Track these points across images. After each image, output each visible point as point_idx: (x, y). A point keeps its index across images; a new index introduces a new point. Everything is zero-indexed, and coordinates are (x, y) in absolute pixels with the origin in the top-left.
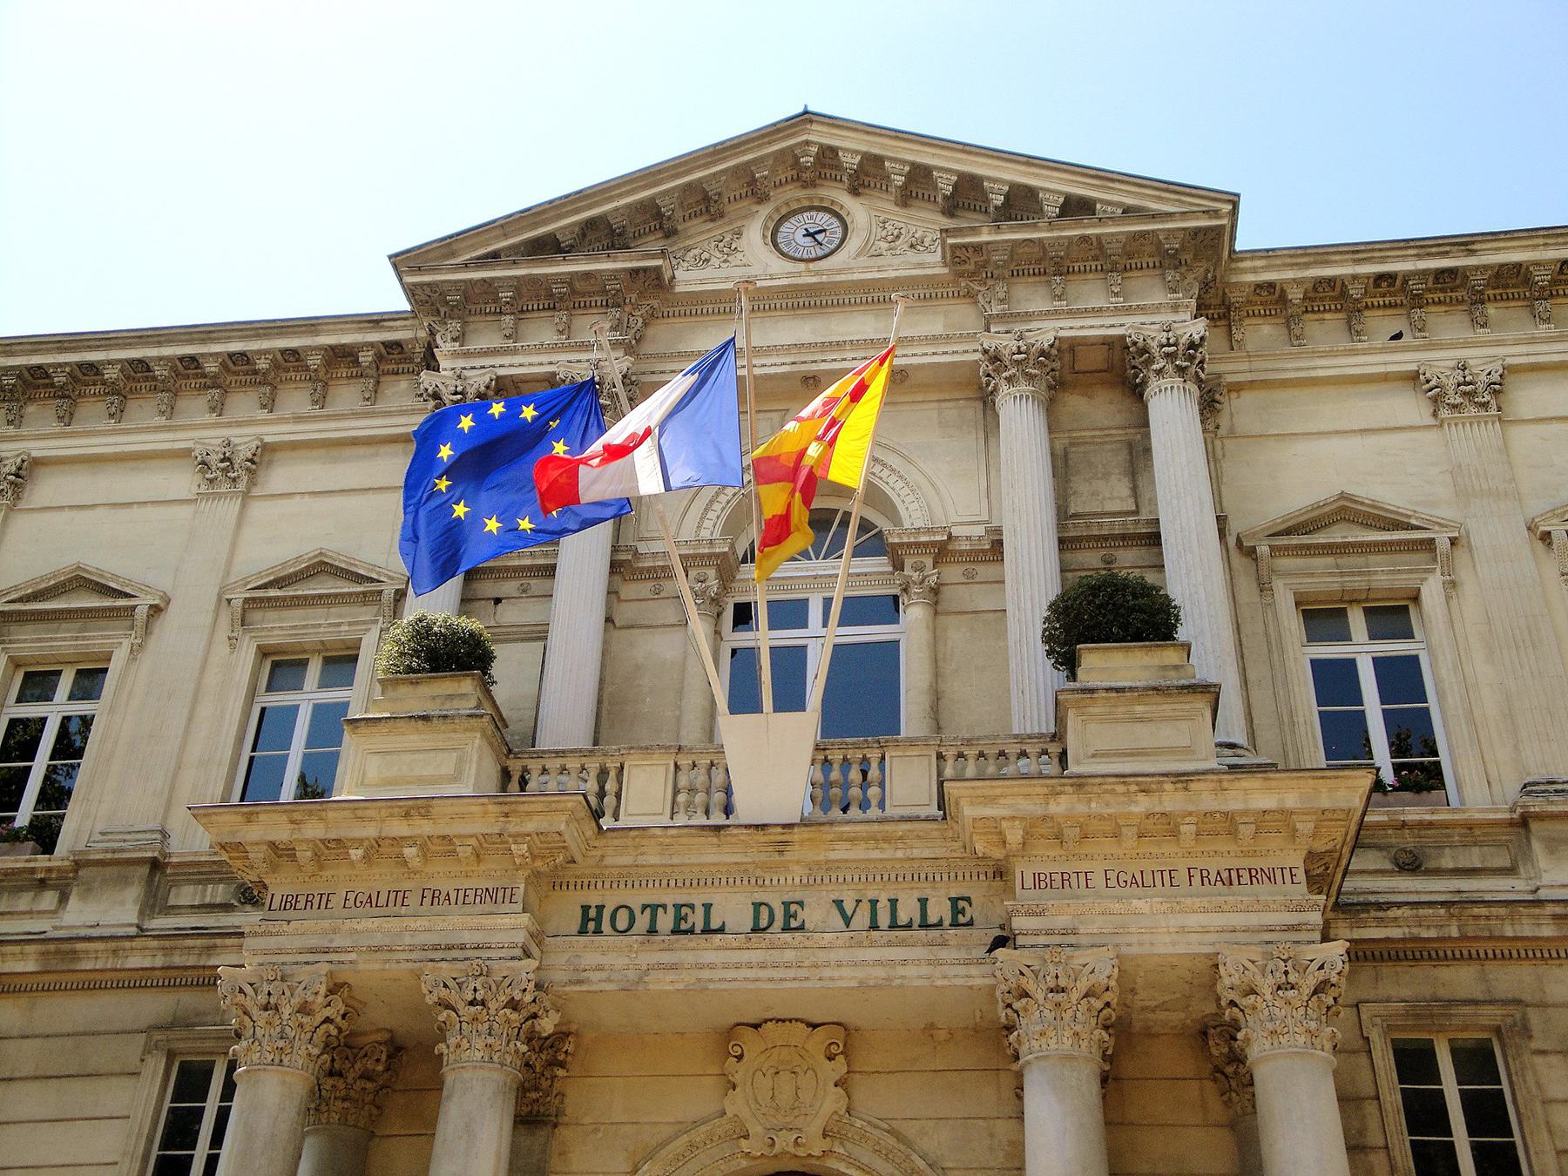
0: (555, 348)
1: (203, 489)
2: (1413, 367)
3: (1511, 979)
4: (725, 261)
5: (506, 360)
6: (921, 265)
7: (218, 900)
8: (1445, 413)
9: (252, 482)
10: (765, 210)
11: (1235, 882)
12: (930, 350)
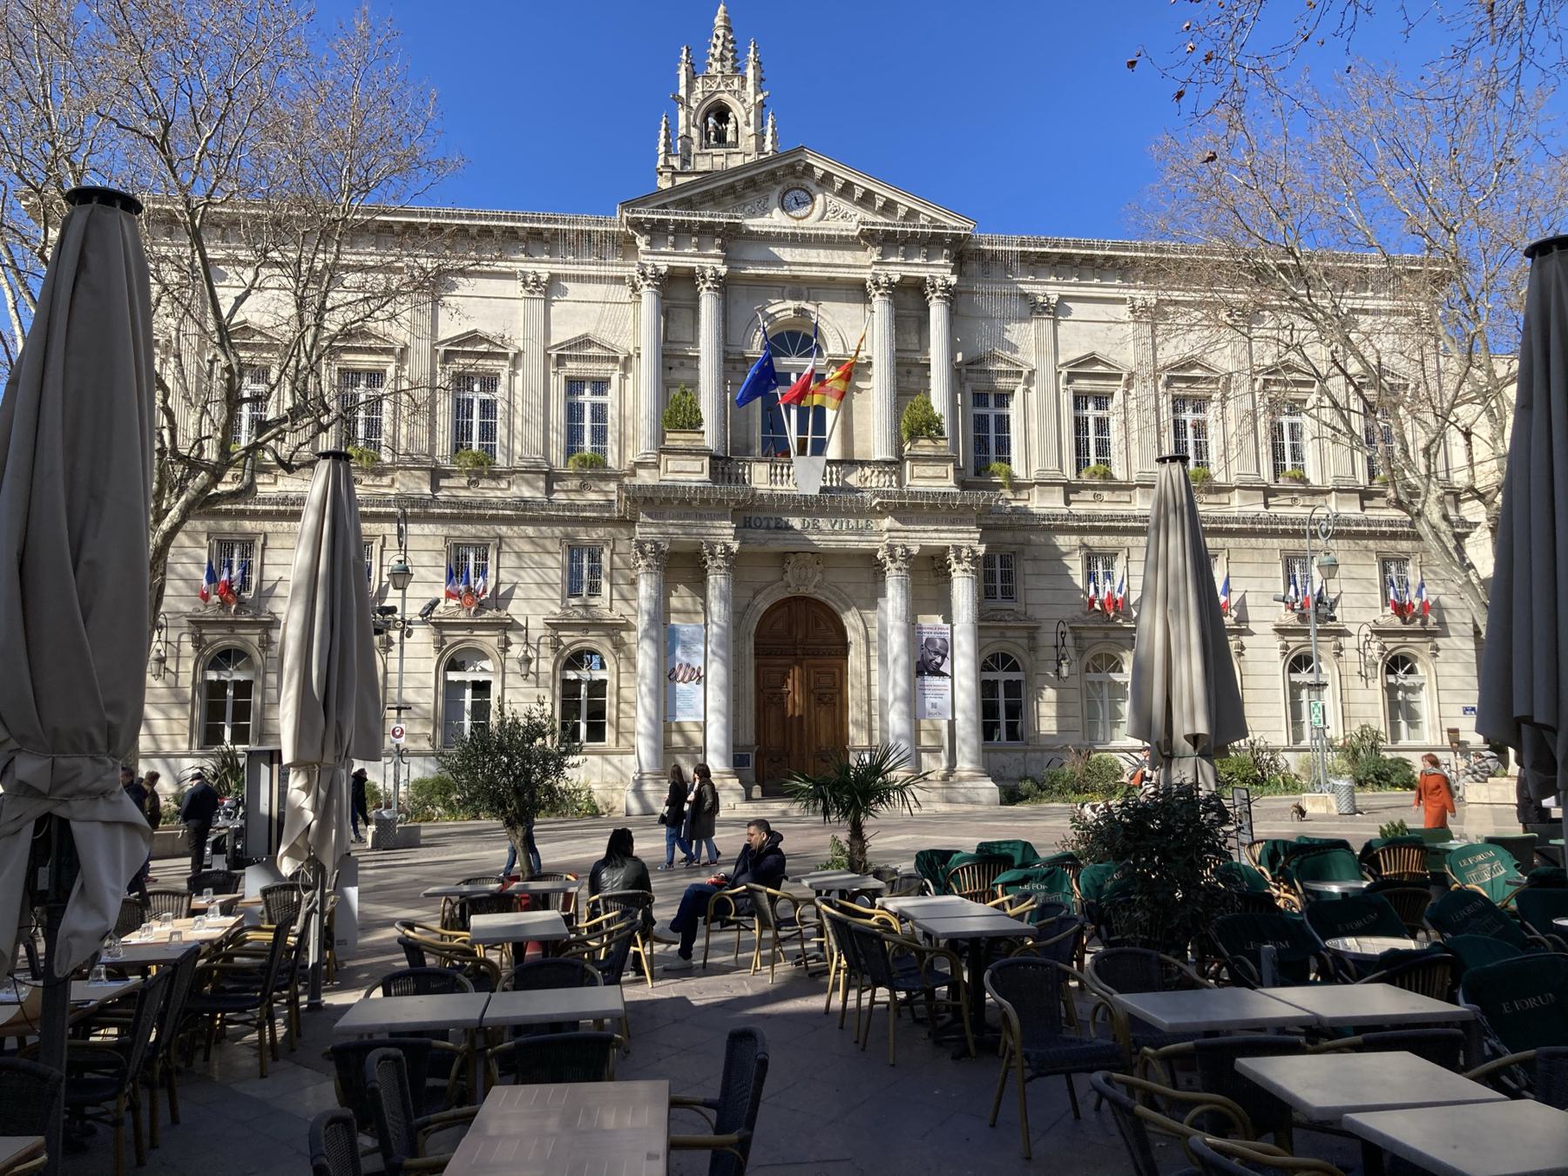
3: (1020, 536)
5: (672, 258)
10: (779, 189)
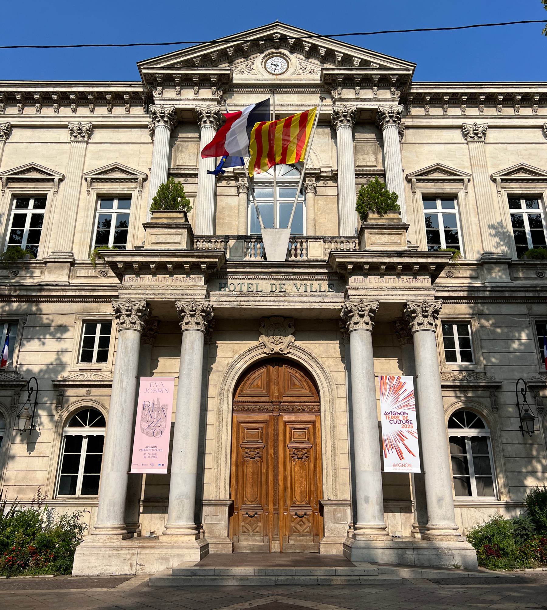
0: (194, 100)
1: (72, 139)
2: (461, 124)
4: (249, 73)
5: (178, 102)
6: (314, 79)
7: (93, 275)
8: (469, 139)
9: (89, 139)
10: (262, 55)
11: (411, 282)
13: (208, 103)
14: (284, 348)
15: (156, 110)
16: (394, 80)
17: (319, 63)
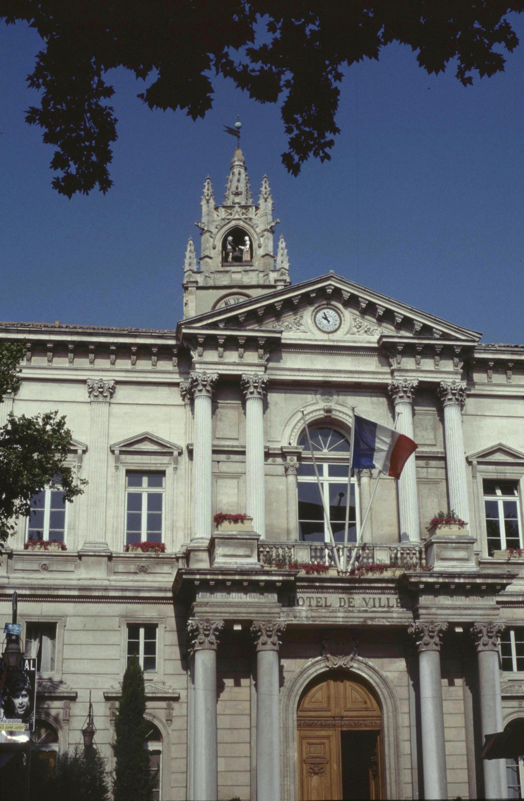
4: (298, 329)
5: (221, 367)
6: (369, 342)
9: (111, 398)
10: (313, 308)
12: (371, 376)
13: (254, 368)
14: (348, 662)
15: (198, 377)
16: (458, 351)
17: (375, 320)
